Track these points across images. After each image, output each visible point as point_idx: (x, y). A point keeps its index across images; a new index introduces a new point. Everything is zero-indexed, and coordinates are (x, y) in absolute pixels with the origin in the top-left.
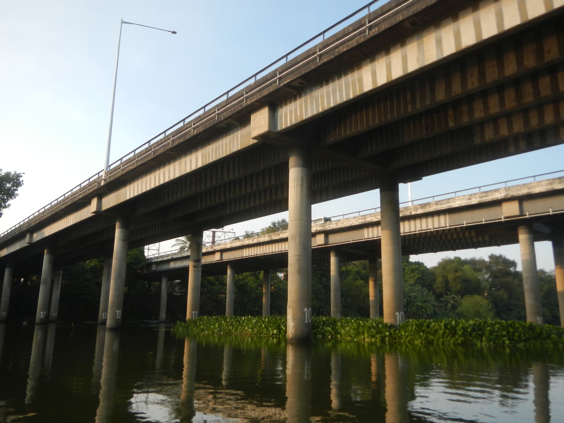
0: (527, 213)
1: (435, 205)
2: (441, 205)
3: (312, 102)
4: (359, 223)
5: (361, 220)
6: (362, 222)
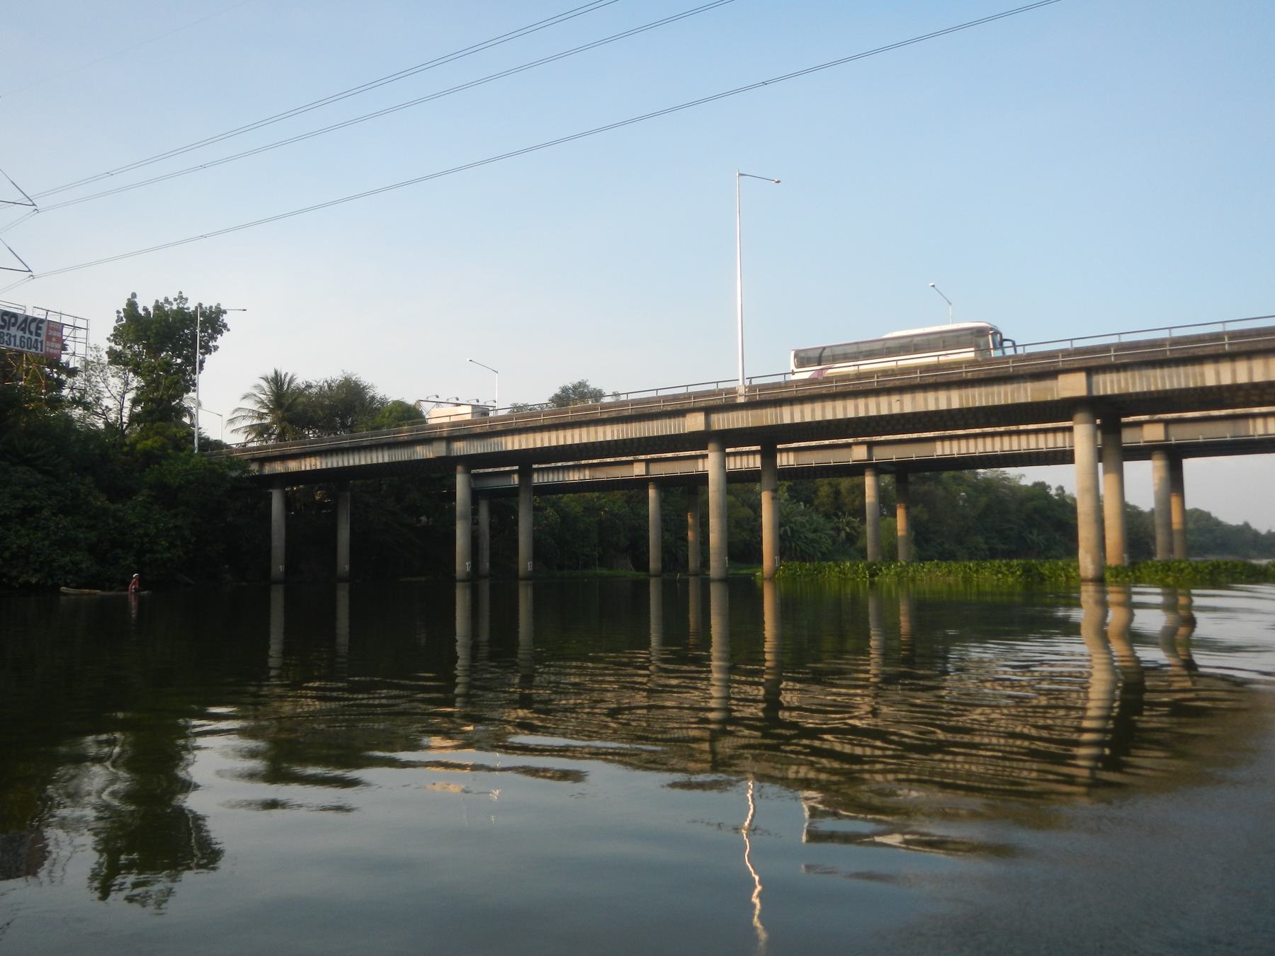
0: (1173, 438)
3: (1141, 379)
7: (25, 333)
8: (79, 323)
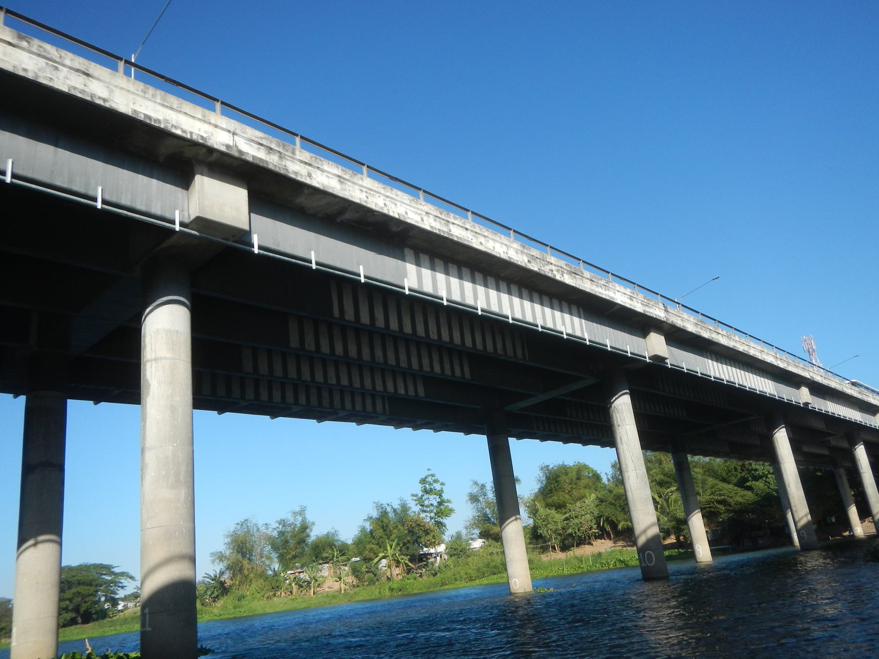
1: (589, 281)
2: (597, 286)
4: (431, 227)
5: (435, 220)
6: (439, 230)
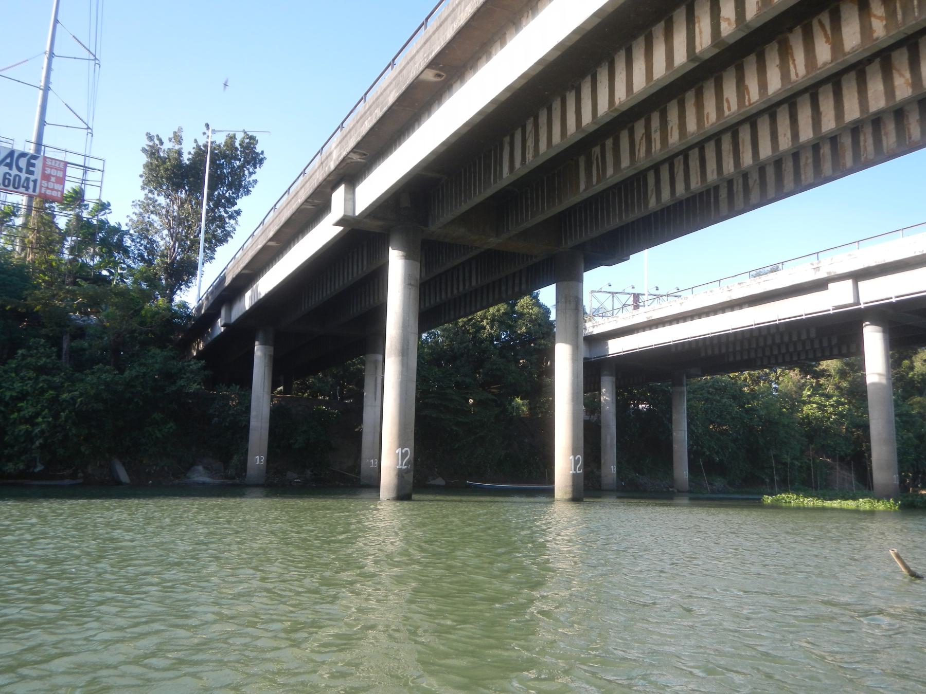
7: (11, 169)
8: (92, 163)
